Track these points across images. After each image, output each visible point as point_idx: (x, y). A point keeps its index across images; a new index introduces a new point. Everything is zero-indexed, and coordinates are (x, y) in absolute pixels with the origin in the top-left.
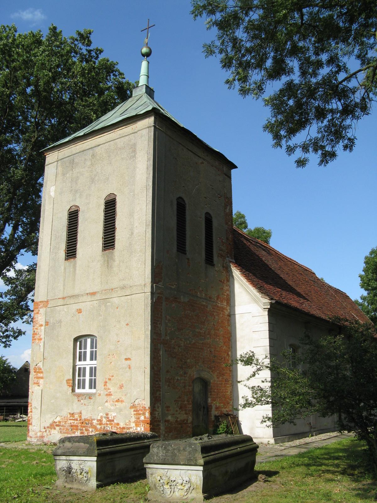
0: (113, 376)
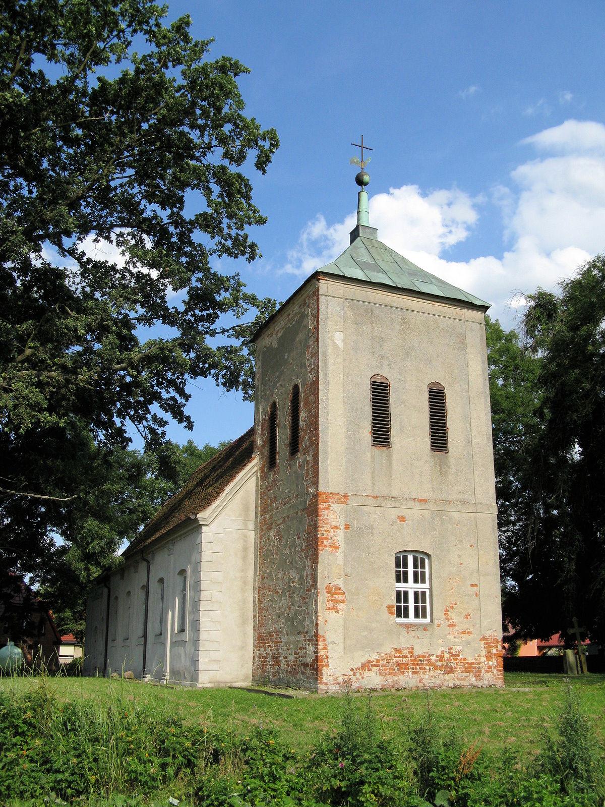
0: (456, 604)
